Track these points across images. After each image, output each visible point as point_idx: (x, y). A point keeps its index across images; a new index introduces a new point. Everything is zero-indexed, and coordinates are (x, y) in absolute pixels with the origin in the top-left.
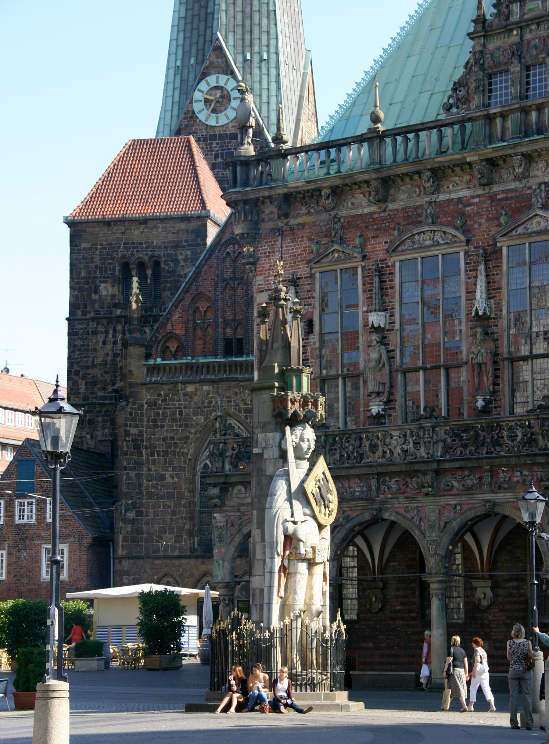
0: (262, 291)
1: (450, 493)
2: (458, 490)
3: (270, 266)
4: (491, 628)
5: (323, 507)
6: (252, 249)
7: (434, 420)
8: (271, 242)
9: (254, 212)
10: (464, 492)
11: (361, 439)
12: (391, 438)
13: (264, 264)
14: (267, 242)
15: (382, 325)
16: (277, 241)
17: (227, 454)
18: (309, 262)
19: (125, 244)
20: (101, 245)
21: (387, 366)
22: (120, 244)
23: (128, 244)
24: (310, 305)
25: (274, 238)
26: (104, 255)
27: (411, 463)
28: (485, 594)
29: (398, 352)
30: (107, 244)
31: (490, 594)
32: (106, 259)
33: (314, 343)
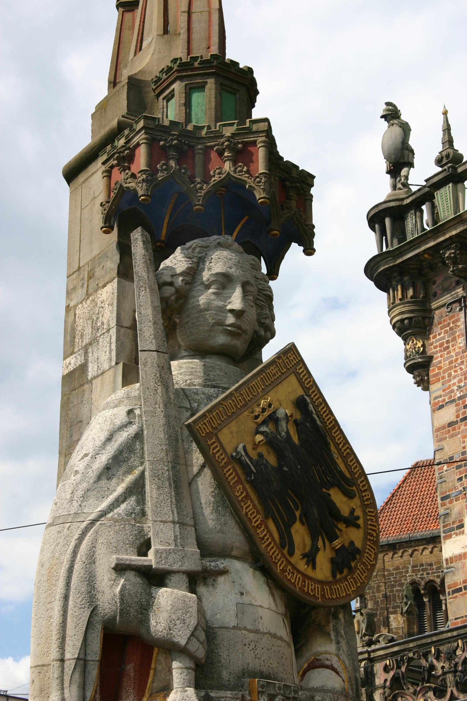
0: (442, 407)
3: (451, 362)
5: (300, 533)
6: (419, 344)
8: (449, 324)
9: (419, 284)
13: (440, 362)
14: (442, 329)
16: (458, 320)
19: (413, 566)
20: (388, 570)
22: (408, 568)
23: (416, 566)
25: (453, 317)
26: (391, 582)
30: (393, 570)
32: (393, 586)
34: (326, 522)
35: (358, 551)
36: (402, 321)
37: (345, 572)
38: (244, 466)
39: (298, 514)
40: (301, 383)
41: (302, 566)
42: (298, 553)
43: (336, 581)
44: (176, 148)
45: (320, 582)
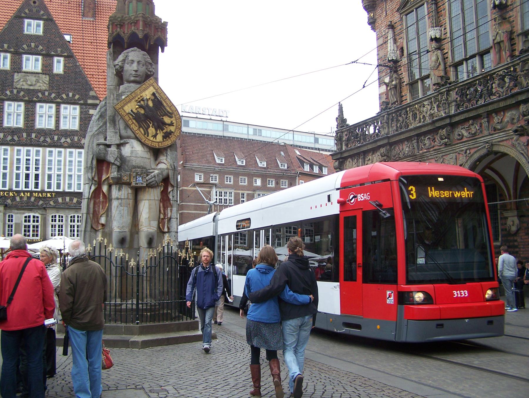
1: (461, 141)
2: (467, 137)
4: (520, 248)
6: (372, 15)
7: (448, 86)
10: (471, 138)
11: (407, 112)
12: (424, 107)
15: (438, 37)
17: (344, 139)
18: (397, 11)
21: (441, 63)
24: (401, 38)
27: (434, 122)
28: (513, 221)
29: (450, 53)
31: (516, 221)
33: (405, 61)
34: (160, 125)
35: (173, 132)
36: (366, 6)
37: (167, 138)
38: (132, 115)
39: (151, 125)
40: (154, 88)
41: (152, 139)
42: (150, 135)
43: (164, 141)
44: (119, 25)
45: (158, 142)
